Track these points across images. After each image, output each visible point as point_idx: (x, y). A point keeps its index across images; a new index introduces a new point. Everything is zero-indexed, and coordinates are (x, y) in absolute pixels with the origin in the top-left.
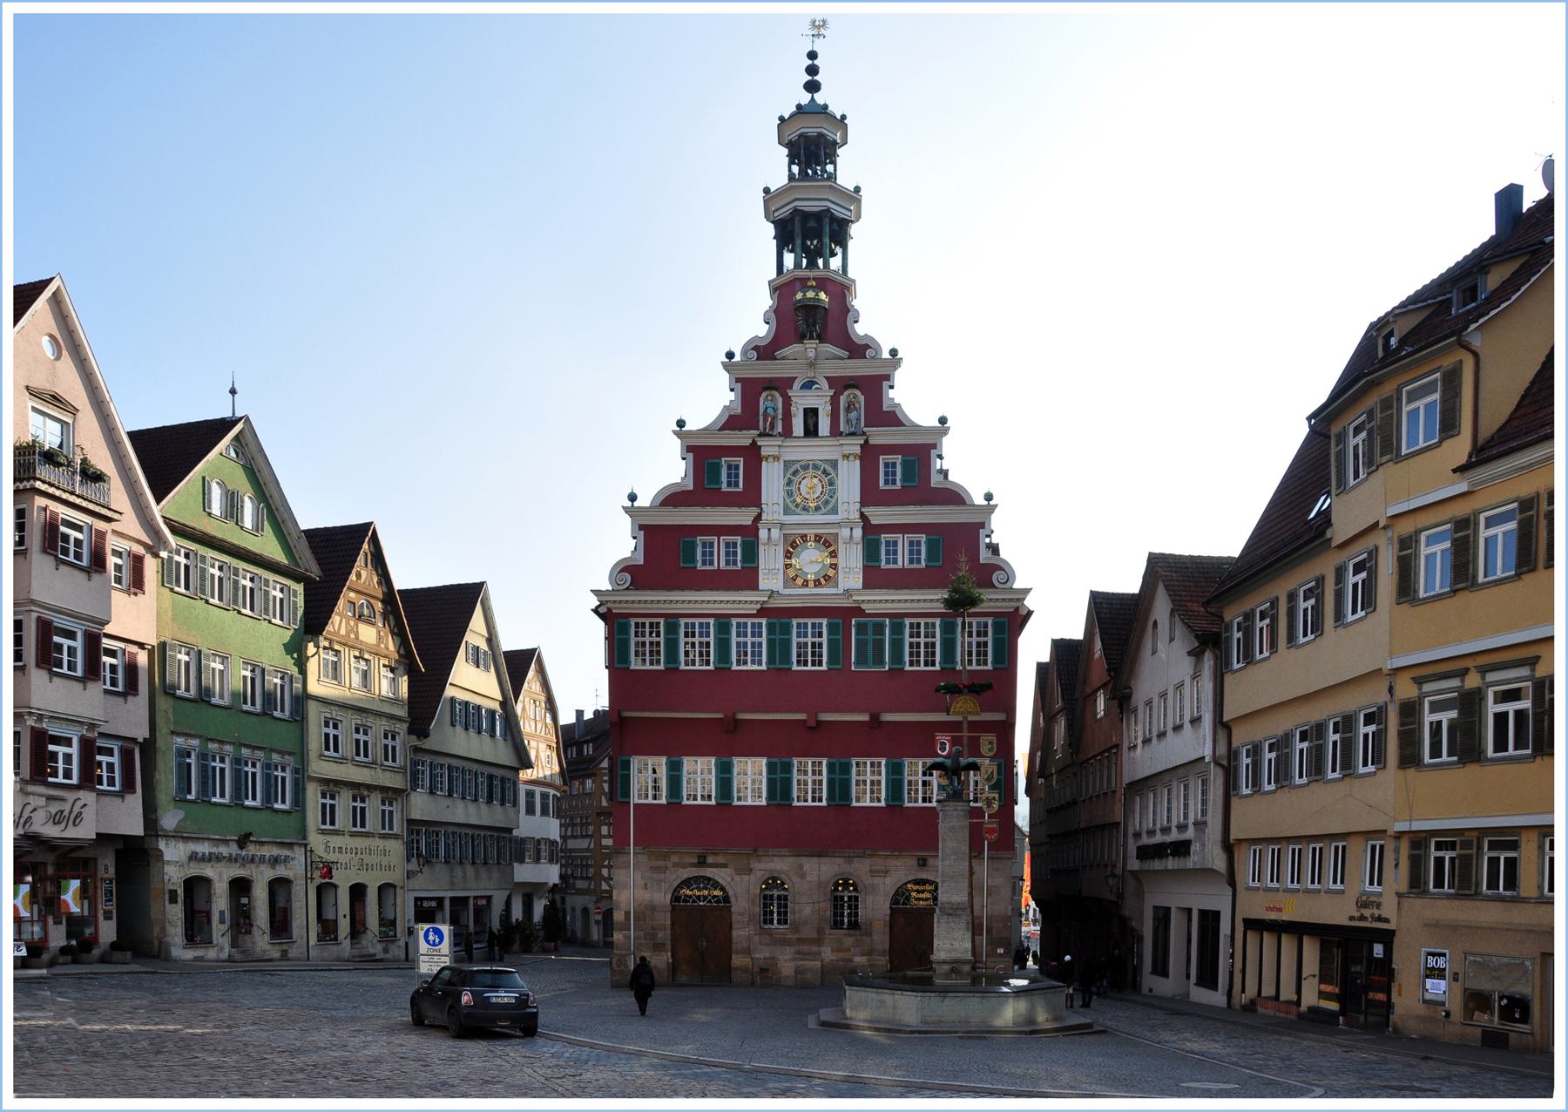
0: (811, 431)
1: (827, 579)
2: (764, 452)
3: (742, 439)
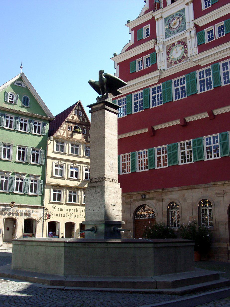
1: (184, 57)
2: (156, 18)
3: (148, 17)
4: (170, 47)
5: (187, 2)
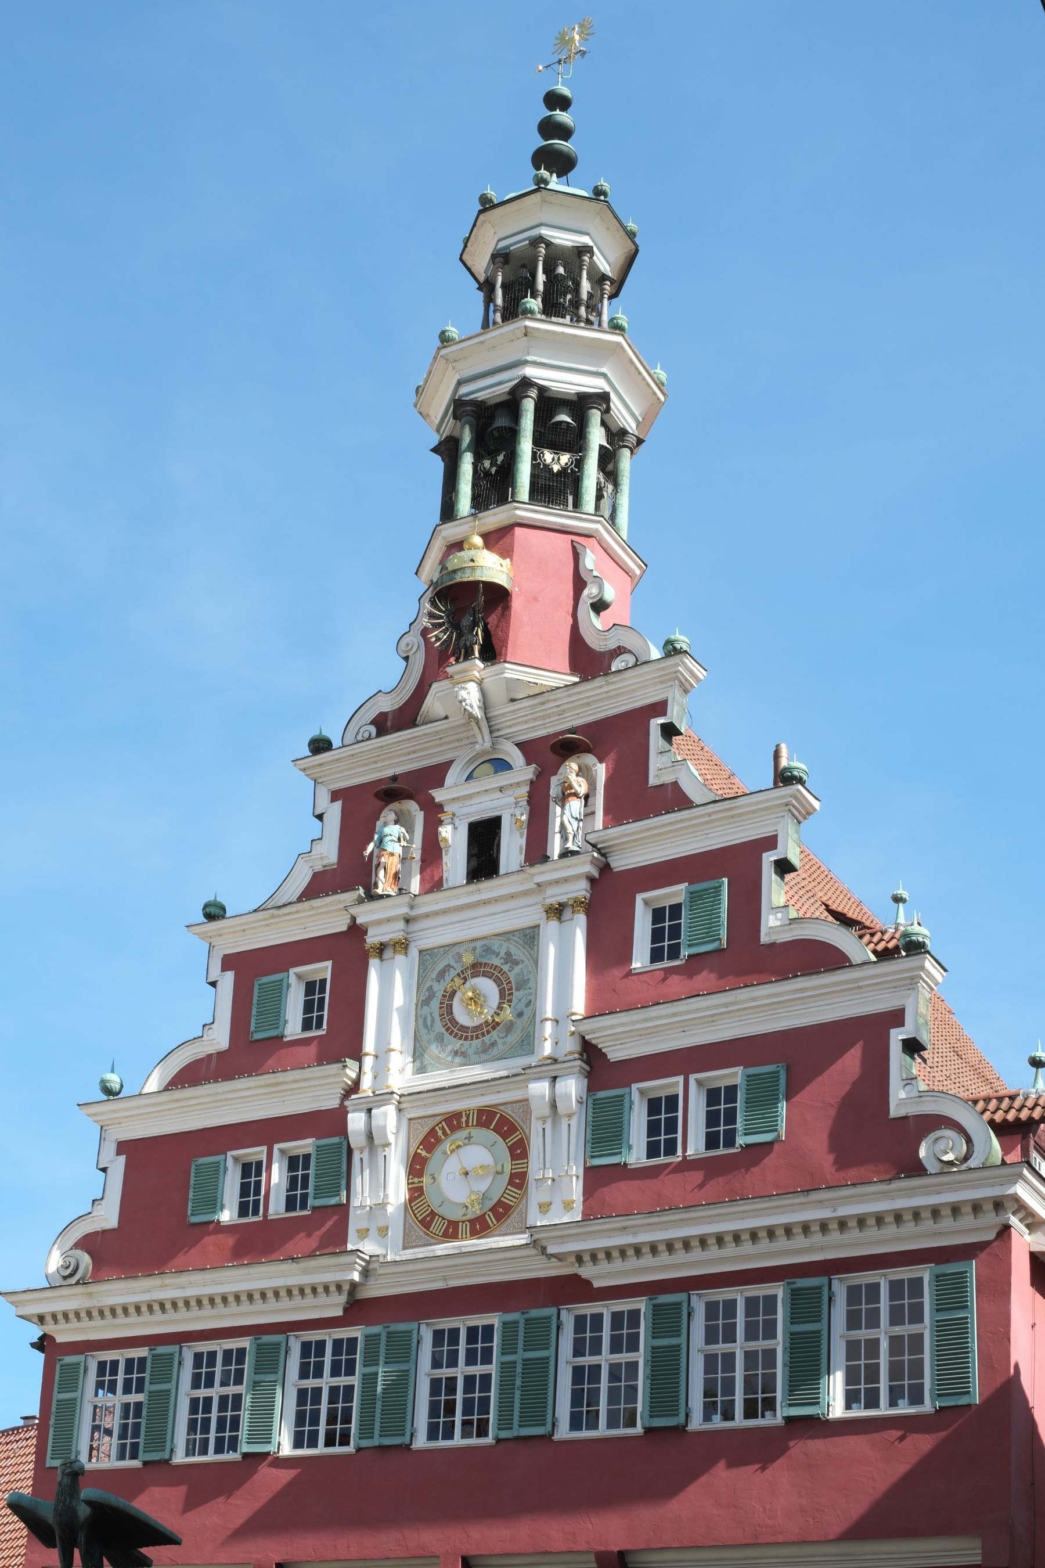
0: (483, 862)
1: (499, 1213)
2: (373, 938)
4: (432, 1132)
5: (554, 901)
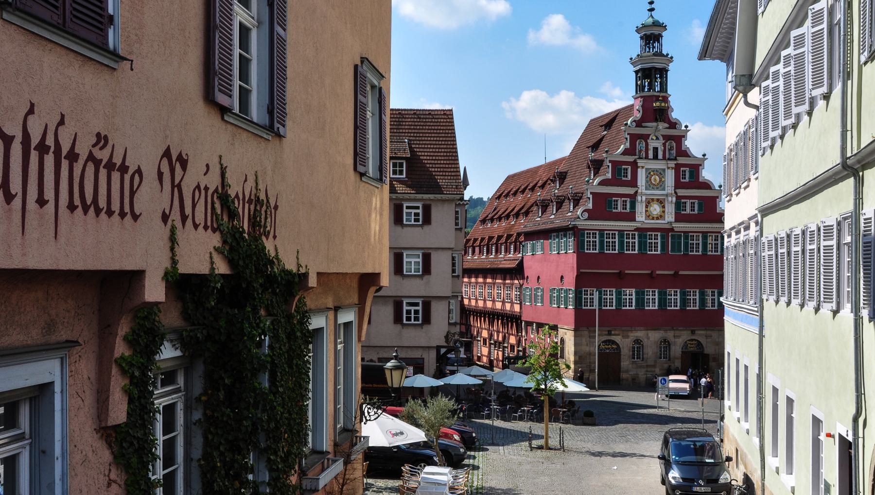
0: (656, 157)
1: (660, 217)
3: (630, 159)
